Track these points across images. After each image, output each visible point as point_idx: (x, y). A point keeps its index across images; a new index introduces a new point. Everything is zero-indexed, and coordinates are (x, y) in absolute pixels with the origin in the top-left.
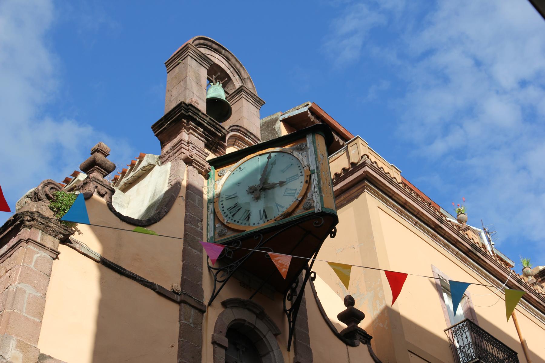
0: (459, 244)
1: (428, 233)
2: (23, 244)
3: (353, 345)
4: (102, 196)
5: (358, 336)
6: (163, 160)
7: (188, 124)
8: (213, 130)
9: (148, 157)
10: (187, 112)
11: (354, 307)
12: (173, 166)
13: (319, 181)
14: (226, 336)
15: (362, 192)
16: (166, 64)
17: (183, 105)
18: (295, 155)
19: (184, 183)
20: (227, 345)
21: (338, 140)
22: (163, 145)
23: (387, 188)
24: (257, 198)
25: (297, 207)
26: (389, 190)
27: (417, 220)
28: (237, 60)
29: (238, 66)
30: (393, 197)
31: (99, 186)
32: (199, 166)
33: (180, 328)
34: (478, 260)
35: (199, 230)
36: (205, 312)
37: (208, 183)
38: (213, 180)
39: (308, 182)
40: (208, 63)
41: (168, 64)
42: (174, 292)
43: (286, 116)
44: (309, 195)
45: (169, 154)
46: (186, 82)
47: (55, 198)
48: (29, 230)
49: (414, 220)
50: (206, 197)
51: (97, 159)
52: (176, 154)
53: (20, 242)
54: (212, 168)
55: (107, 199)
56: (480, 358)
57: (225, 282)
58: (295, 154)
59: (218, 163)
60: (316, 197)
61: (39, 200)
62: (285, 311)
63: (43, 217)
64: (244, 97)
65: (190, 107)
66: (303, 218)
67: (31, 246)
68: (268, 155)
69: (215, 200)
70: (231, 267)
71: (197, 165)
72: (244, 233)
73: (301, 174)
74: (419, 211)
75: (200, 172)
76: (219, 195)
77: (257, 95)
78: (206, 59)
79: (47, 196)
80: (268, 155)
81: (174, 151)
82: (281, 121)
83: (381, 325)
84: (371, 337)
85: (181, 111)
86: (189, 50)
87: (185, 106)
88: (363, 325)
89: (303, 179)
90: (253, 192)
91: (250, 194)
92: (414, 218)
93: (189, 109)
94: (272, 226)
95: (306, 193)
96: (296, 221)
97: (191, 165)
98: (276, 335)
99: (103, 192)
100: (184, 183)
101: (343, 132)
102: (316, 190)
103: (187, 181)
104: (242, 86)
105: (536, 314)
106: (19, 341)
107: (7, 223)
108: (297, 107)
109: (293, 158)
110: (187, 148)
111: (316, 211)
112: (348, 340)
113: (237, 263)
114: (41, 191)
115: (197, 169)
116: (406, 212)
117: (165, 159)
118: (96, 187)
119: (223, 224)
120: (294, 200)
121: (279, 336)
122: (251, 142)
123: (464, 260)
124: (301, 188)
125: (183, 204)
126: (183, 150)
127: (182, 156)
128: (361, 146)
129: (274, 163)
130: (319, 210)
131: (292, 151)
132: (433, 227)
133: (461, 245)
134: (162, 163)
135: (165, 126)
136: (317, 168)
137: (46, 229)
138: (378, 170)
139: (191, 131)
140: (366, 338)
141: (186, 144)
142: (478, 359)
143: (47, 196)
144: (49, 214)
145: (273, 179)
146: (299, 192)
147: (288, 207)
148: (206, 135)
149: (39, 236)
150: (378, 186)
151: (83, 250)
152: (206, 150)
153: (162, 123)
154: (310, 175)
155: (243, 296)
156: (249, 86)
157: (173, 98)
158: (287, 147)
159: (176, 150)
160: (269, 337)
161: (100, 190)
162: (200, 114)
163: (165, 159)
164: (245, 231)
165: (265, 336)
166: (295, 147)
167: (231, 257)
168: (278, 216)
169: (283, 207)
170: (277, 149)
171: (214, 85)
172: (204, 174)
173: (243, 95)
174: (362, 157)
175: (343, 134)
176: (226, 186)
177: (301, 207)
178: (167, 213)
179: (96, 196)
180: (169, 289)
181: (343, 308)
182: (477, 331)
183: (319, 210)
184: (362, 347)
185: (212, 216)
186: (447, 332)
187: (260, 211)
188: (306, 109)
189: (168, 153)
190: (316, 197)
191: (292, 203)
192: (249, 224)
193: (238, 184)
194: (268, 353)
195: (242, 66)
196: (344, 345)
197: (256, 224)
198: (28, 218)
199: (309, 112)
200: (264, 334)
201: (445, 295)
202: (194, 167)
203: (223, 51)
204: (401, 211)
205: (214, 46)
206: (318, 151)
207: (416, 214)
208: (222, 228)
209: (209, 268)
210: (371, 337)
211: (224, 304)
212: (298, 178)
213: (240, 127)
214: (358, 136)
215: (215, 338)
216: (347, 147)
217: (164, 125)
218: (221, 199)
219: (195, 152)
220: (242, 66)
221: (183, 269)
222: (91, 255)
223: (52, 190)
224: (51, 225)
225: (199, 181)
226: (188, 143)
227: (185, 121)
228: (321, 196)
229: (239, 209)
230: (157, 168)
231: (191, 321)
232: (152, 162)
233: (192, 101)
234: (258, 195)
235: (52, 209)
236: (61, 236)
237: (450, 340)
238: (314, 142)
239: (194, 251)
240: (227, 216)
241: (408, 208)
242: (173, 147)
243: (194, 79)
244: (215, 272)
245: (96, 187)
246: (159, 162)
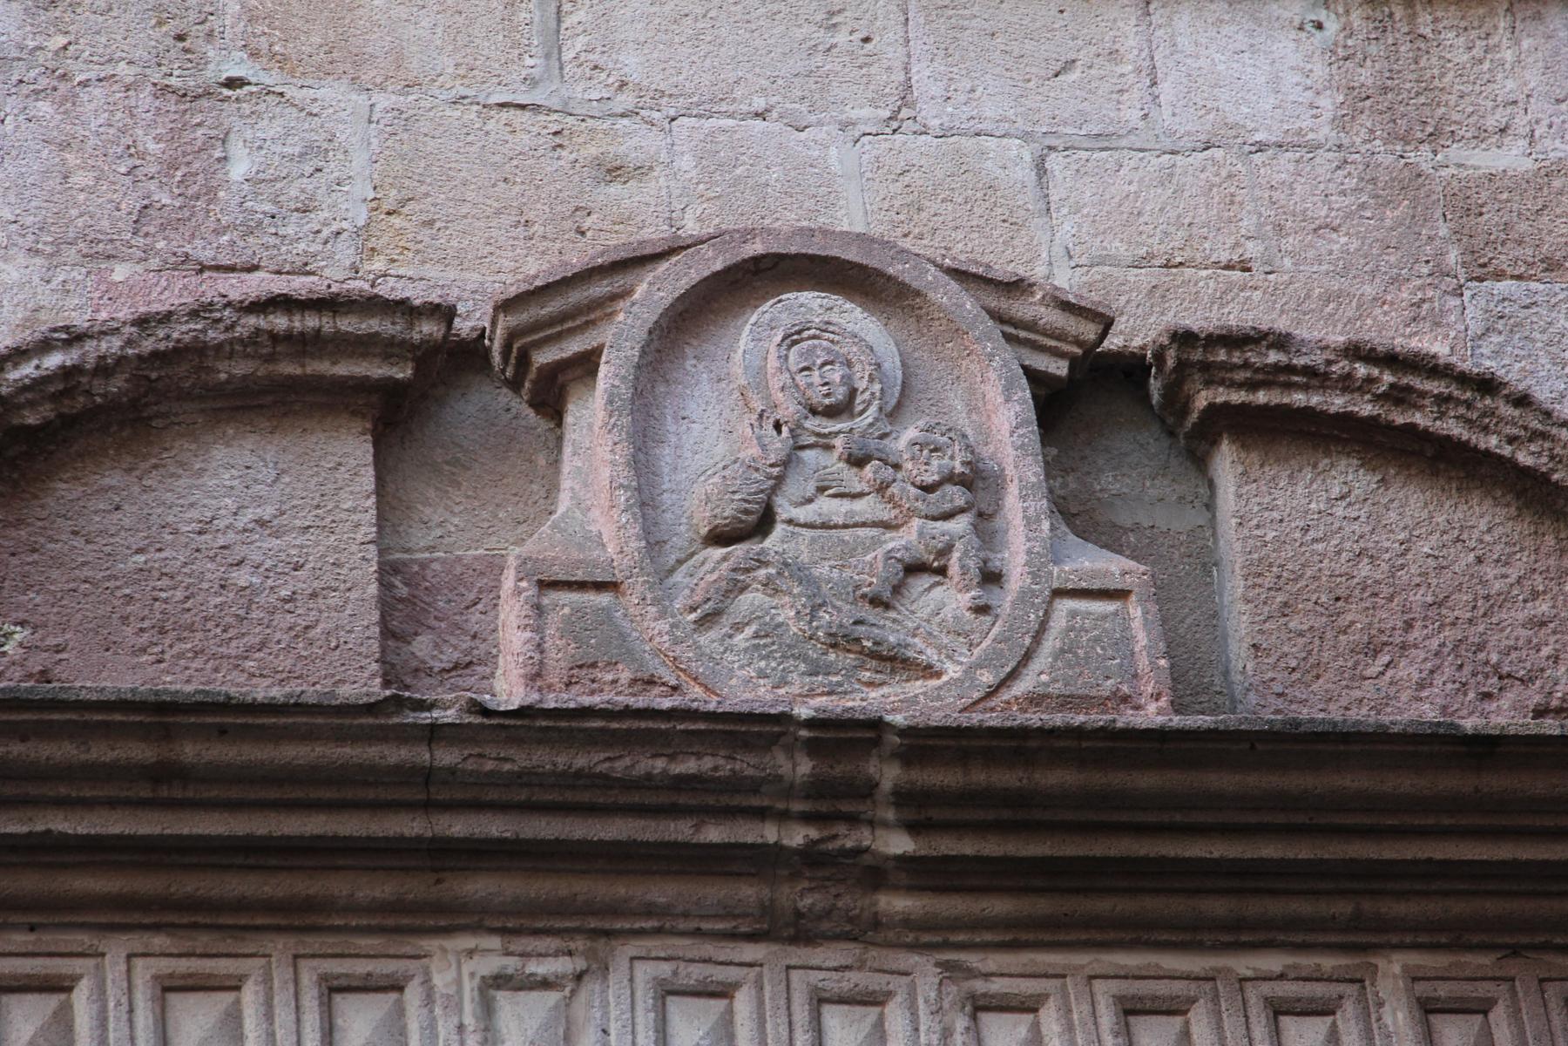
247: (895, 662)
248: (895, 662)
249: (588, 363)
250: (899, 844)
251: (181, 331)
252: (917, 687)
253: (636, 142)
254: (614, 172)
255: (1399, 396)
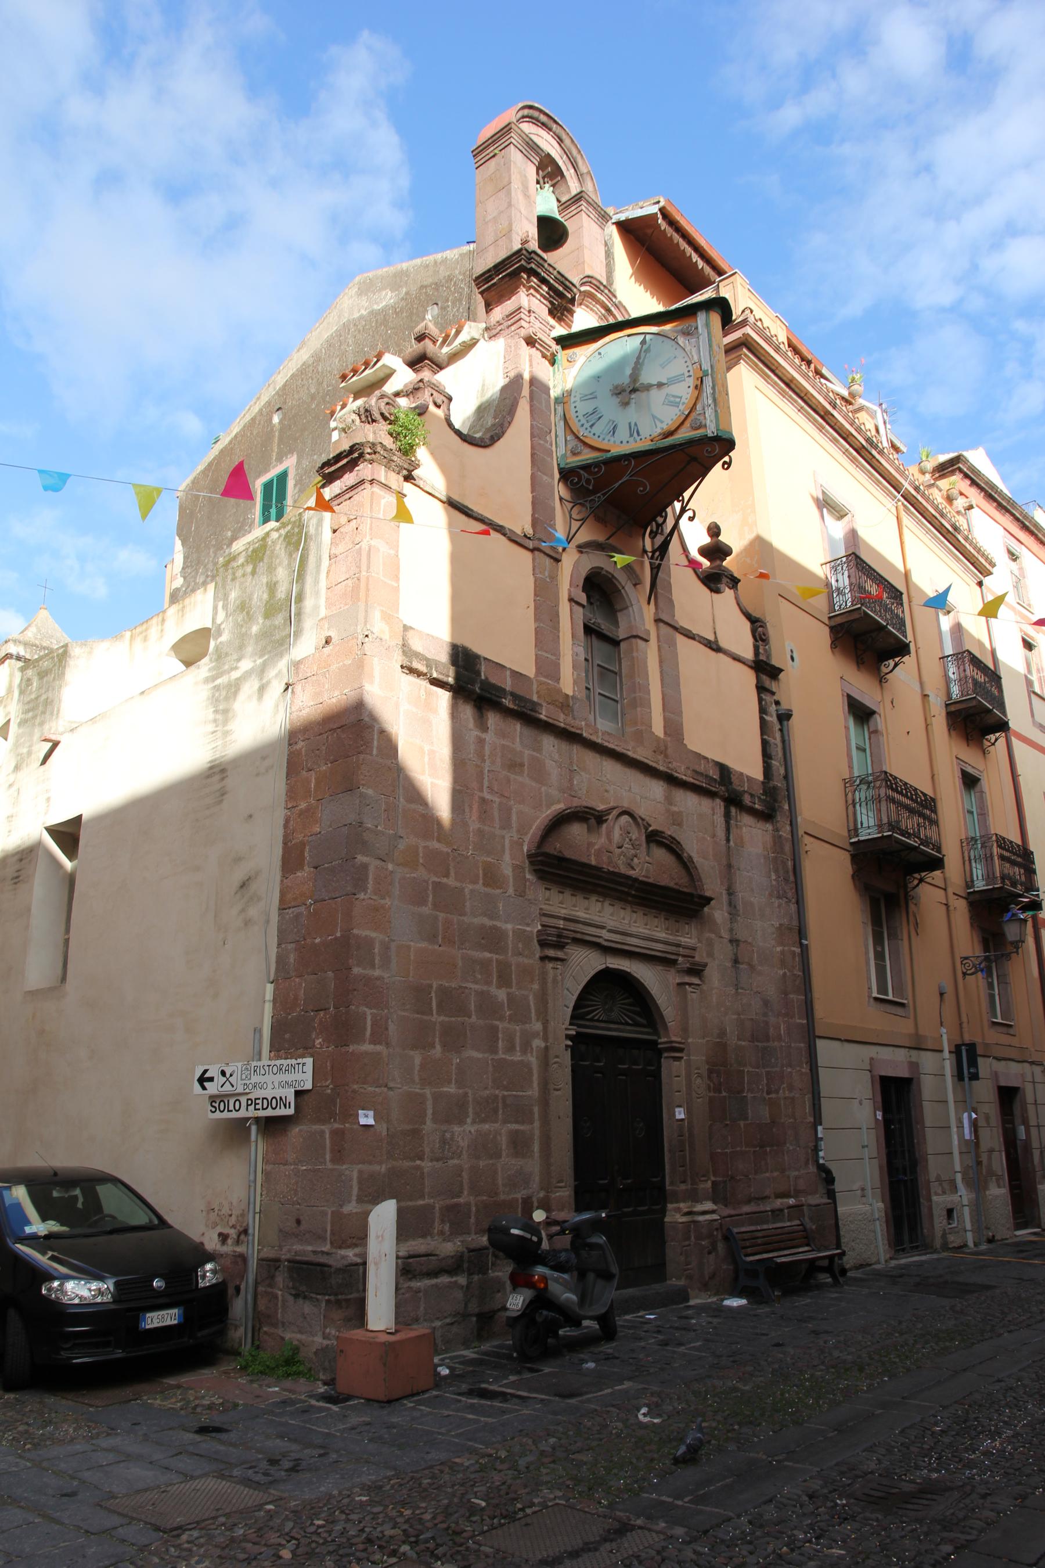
0: (851, 437)
1: (814, 422)
2: (367, 485)
3: (717, 591)
4: (439, 407)
5: (724, 580)
6: (492, 332)
7: (528, 281)
8: (561, 289)
9: (470, 327)
10: (529, 263)
11: (720, 538)
12: (508, 347)
13: (713, 388)
14: (583, 591)
15: (737, 363)
16: (474, 153)
17: (524, 252)
18: (680, 343)
19: (527, 376)
20: (584, 601)
21: (691, 256)
22: (489, 307)
23: (770, 359)
24: (625, 404)
25: (682, 423)
26: (773, 362)
27: (803, 404)
28: (572, 141)
29: (574, 152)
30: (777, 371)
31: (435, 393)
32: (544, 348)
33: (535, 583)
34: (872, 461)
35: (548, 445)
36: (560, 561)
37: (554, 370)
38: (560, 368)
39: (699, 387)
40: (537, 154)
41: (477, 152)
42: (525, 536)
43: (622, 217)
44: (699, 407)
45: (502, 326)
46: (509, 193)
47: (392, 418)
48: (370, 466)
49: (799, 405)
50: (554, 393)
51: (428, 351)
52: (513, 328)
53: (362, 482)
54: (559, 347)
55: (444, 411)
56: (862, 605)
57: (583, 520)
58: (681, 340)
59: (568, 342)
60: (709, 413)
61: (374, 421)
62: (645, 551)
63: (385, 449)
64: (584, 209)
65: (533, 255)
66: (691, 443)
67: (376, 489)
68: (642, 337)
69: (565, 400)
70: (590, 501)
71: (541, 346)
72: (609, 455)
73: (688, 374)
74: (807, 392)
75: (544, 356)
76: (569, 393)
77: (600, 204)
78: (535, 147)
79: (382, 414)
80: (642, 337)
81: (510, 323)
82: (613, 223)
83: (748, 560)
84: (739, 581)
85: (520, 261)
86: (512, 134)
87: (527, 254)
88: (727, 562)
89: (691, 382)
90: (620, 393)
91: (615, 397)
92: (800, 401)
93: (532, 258)
94: (647, 448)
95: (695, 404)
96: (681, 445)
97: (534, 346)
98: (635, 585)
99: (439, 402)
100: (527, 376)
101: (705, 247)
102: (710, 402)
103: (531, 372)
104: (582, 192)
105: (928, 531)
106: (382, 611)
107: (341, 453)
108: (641, 204)
109: (677, 346)
110: (527, 319)
111: (710, 435)
112: (712, 585)
113: (599, 497)
114: (375, 409)
115: (541, 351)
116: (791, 393)
117: (494, 332)
118: (432, 395)
119: (577, 437)
120: (679, 413)
121: (638, 586)
122: (604, 300)
123: (853, 460)
124: (688, 396)
125: (527, 408)
126: (523, 323)
127: (523, 332)
128: (739, 286)
129: (647, 351)
130: (713, 433)
131: (676, 335)
132: (822, 414)
133: (853, 439)
134: (490, 338)
135: (495, 280)
136: (711, 366)
137: (388, 463)
138: (760, 332)
139: (532, 291)
140: (734, 582)
141: (527, 313)
142: (859, 606)
143: (382, 414)
144: (388, 442)
145: (648, 376)
146: (686, 401)
147: (670, 422)
148: (550, 296)
149: (382, 473)
150: (759, 355)
151: (426, 489)
152: (552, 322)
153: (490, 276)
154: (702, 378)
155: (601, 538)
156: (589, 187)
157: (489, 217)
158: (668, 327)
159: (512, 321)
160: (629, 587)
161: (436, 399)
162: (546, 265)
163: (494, 332)
164: (609, 451)
165: (623, 588)
166: (680, 328)
167: (591, 488)
168: (656, 434)
169: (662, 422)
170: (654, 329)
171: (541, 188)
172: (549, 358)
173: (583, 207)
174: (743, 311)
175: (704, 250)
176: (580, 379)
177: (687, 424)
178: (510, 423)
179: (432, 408)
180: (519, 532)
181: (706, 540)
182: (863, 568)
183: (713, 433)
184: (728, 594)
185: (562, 423)
186: (824, 566)
187: (630, 424)
188: (655, 209)
189: (499, 323)
190: (709, 413)
191: (675, 418)
192: (615, 442)
193: (597, 378)
194: (627, 608)
195: (579, 152)
196: (708, 591)
197: (625, 442)
198: (369, 450)
199: (659, 215)
200: (623, 584)
201: (825, 510)
202: (538, 349)
203: (554, 126)
204: (784, 391)
205: (543, 118)
206: (713, 339)
207: (802, 395)
208: (575, 442)
209: (561, 499)
210: (739, 581)
211: (581, 548)
212: (684, 380)
213: (592, 277)
214: (736, 270)
215: (573, 595)
216: (718, 285)
217: (493, 279)
218: (573, 399)
219: (538, 324)
220: (579, 152)
221: (533, 503)
222: (437, 495)
223: (388, 406)
224: (395, 458)
225: (544, 371)
226: (529, 311)
227: (525, 276)
228: (716, 411)
229: (600, 418)
230: (482, 344)
231: (547, 574)
232: (477, 337)
233: (528, 236)
234: (627, 400)
235: (391, 434)
236: (405, 472)
237: (827, 578)
238: (707, 325)
239: (545, 478)
240: (582, 425)
241: (793, 386)
242: (507, 316)
243: (520, 186)
244: (570, 505)
245: (432, 395)
246: (486, 335)
247: (633, 868)
248: (633, 868)
249: (607, 820)
250: (633, 892)
251: (579, 809)
252: (634, 872)
253: (608, 788)
254: (607, 791)
255: (672, 842)
